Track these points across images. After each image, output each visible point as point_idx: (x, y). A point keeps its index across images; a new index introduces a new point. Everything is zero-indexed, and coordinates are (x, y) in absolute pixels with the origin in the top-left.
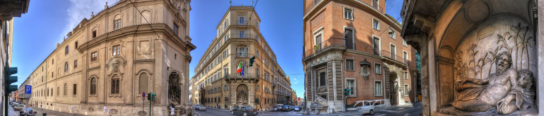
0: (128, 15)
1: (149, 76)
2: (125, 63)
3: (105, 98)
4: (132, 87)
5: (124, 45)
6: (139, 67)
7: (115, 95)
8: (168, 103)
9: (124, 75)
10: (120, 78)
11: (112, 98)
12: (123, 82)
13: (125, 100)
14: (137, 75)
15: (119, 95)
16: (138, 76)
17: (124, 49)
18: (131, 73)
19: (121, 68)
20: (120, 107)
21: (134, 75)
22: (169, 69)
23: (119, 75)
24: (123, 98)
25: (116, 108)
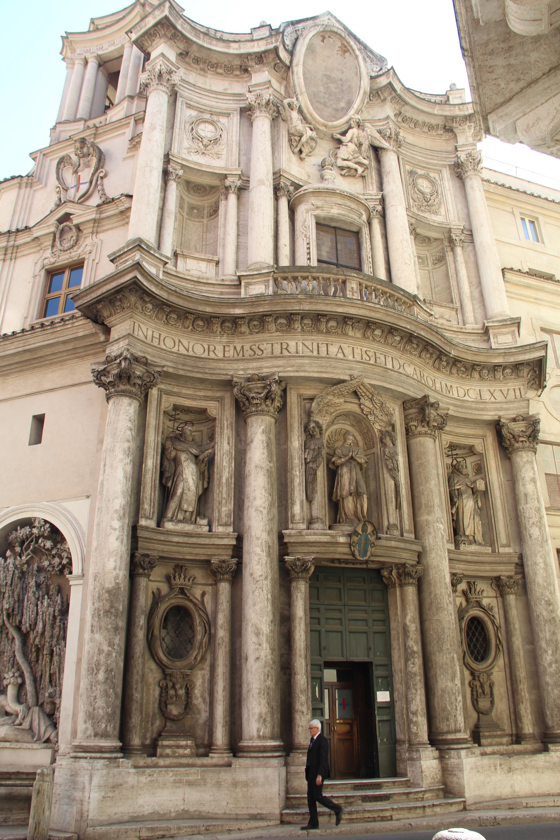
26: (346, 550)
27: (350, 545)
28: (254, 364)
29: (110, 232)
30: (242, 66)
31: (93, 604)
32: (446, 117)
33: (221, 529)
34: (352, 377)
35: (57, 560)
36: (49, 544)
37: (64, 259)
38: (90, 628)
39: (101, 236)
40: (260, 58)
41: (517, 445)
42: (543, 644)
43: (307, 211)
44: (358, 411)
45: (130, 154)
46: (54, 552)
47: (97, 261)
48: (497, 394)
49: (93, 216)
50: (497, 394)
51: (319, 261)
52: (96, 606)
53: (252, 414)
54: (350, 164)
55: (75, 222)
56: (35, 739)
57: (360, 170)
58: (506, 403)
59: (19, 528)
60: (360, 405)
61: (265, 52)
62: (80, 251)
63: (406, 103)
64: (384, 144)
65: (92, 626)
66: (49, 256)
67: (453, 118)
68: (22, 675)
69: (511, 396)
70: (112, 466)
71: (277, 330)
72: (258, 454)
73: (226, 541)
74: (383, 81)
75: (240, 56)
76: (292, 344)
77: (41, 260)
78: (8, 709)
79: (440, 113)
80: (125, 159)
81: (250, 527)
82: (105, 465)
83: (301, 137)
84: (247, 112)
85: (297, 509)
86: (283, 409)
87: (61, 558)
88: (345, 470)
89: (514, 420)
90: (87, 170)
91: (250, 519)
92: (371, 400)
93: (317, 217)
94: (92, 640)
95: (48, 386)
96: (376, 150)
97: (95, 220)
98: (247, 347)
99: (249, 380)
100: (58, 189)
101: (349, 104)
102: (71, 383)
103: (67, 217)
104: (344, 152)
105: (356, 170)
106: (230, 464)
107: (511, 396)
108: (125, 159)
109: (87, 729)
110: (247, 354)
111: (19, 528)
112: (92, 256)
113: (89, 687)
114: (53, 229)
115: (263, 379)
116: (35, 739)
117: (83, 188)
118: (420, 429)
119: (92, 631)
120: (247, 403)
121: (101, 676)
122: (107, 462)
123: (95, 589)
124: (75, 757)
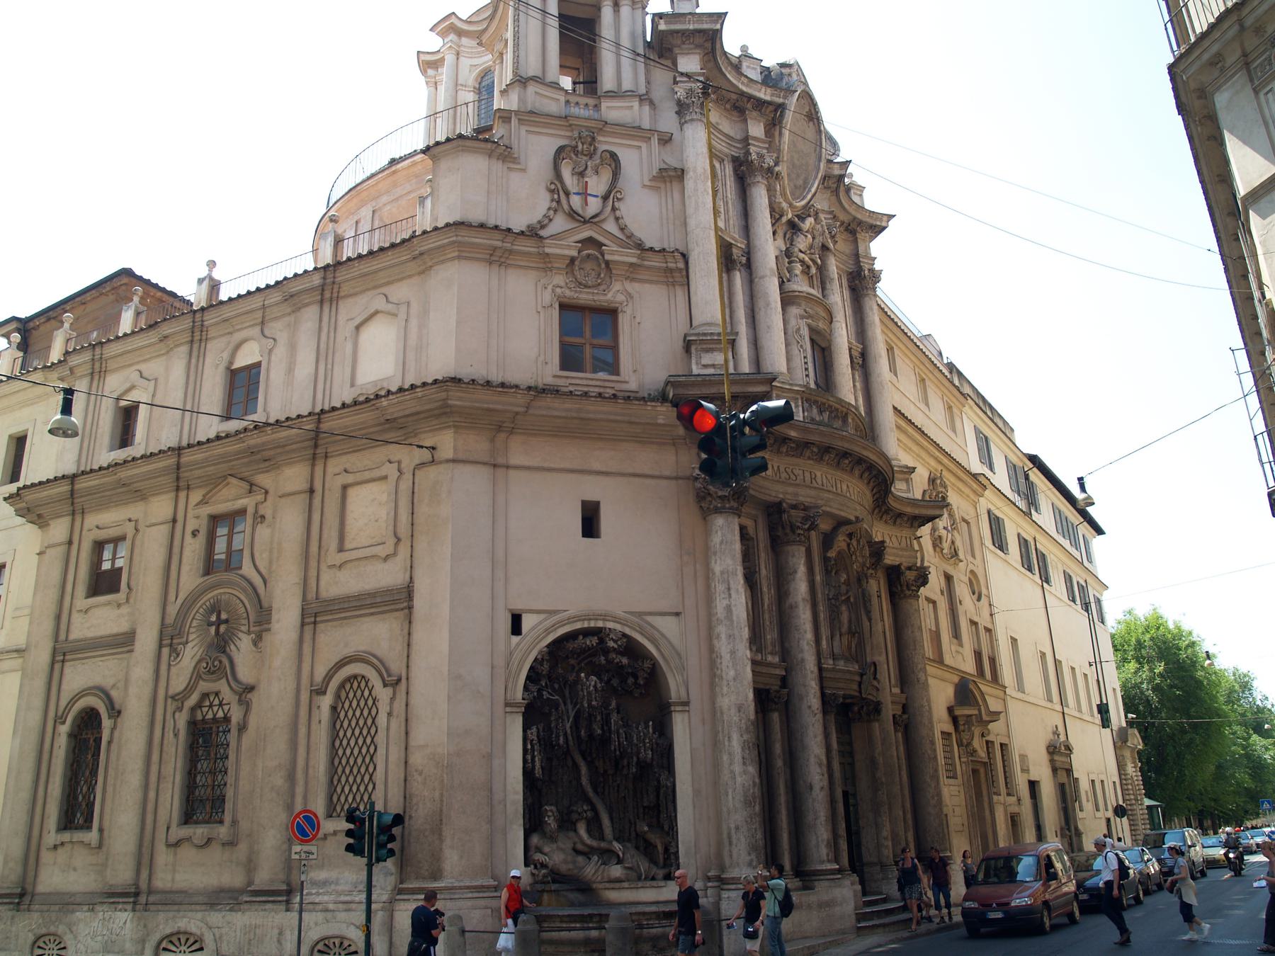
0: (293, 347)
1: (383, 694)
2: (263, 616)
3: (144, 858)
4: (291, 778)
5: (266, 510)
6: (337, 641)
7: (200, 832)
9: (254, 697)
10: (236, 715)
11: (187, 852)
12: (247, 739)
13: (250, 866)
14: (322, 692)
15: (223, 831)
16: (326, 701)
17: (263, 532)
18: (291, 685)
19: (243, 649)
20: (215, 918)
21: (305, 696)
22: (527, 622)
23: (227, 694)
24: (243, 848)
25: (191, 922)
26: (855, 687)
27: (860, 684)
28: (790, 489)
29: (647, 286)
30: (740, 105)
32: (855, 218)
33: (770, 658)
34: (857, 518)
35: (631, 680)
36: (625, 661)
37: (585, 297)
39: (637, 286)
40: (760, 104)
41: (908, 593)
42: (928, 780)
43: (802, 317)
44: (845, 548)
45: (653, 184)
47: (638, 320)
48: (894, 539)
49: (634, 260)
50: (894, 539)
51: (816, 383)
52: (746, 737)
53: (789, 543)
54: (807, 259)
55: (607, 257)
57: (813, 270)
58: (902, 549)
60: (848, 545)
61: (770, 103)
62: (609, 296)
63: (838, 196)
64: (831, 246)
66: (563, 284)
67: (860, 223)
68: (594, 809)
69: (903, 544)
70: (737, 591)
71: (809, 458)
72: (800, 588)
73: (778, 672)
74: (837, 172)
75: (742, 94)
76: (819, 474)
77: (550, 287)
78: (579, 847)
79: (853, 213)
80: (644, 186)
81: (803, 660)
82: (729, 589)
83: (781, 216)
84: (744, 171)
85: (824, 643)
86: (809, 539)
87: (636, 677)
88: (844, 608)
89: (909, 568)
90: (595, 177)
91: (802, 651)
92: (858, 542)
93: (809, 326)
94: (745, 772)
95: (597, 466)
96: (824, 248)
97: (632, 265)
98: (782, 469)
99: (794, 507)
100: (553, 187)
101: (805, 186)
102: (631, 471)
103: (590, 242)
104: (802, 243)
105: (808, 267)
106: (769, 590)
107: (903, 544)
108: (644, 186)
109: (752, 861)
110: (784, 475)
112: (629, 310)
114: (574, 253)
115: (806, 509)
117: (594, 205)
118: (870, 571)
119: (744, 764)
120: (788, 531)
121: (757, 808)
122: (732, 586)
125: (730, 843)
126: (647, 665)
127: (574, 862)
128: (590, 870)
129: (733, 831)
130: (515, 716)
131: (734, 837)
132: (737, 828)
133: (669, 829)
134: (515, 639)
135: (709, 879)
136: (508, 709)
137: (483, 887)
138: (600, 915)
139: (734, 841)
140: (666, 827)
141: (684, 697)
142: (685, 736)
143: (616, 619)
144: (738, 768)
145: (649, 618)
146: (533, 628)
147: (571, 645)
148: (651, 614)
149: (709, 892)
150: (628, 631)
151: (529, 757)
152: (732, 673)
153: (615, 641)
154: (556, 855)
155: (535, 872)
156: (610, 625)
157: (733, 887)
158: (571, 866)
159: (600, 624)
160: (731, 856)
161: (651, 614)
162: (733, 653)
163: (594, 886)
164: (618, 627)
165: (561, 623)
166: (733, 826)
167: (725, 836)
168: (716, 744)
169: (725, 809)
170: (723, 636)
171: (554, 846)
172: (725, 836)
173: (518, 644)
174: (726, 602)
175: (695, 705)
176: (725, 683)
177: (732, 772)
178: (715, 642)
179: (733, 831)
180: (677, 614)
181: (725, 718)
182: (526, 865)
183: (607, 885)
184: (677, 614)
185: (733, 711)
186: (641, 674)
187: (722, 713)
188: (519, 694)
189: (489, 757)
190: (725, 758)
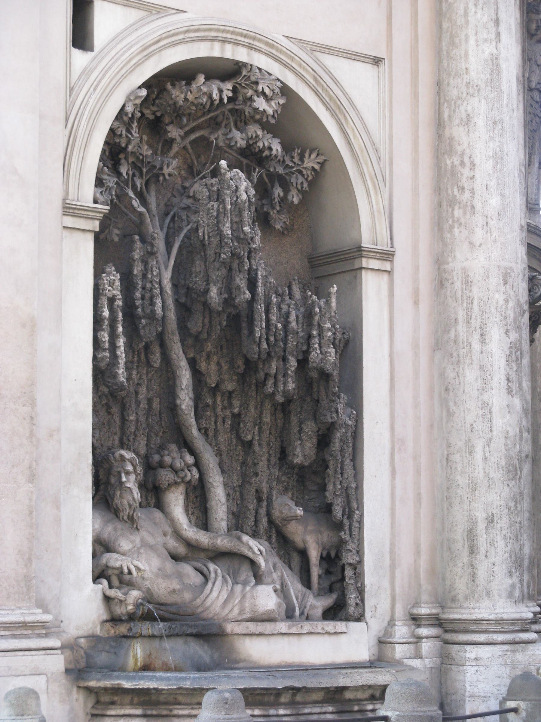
8: (82, 607)
31: (507, 333)
38: (504, 383)
46: (280, 170)
52: (514, 336)
56: (297, 613)
59: (201, 79)
65: (508, 380)
82: (497, 22)
87: (286, 186)
109: (513, 586)
111: (201, 79)
113: (512, 504)
116: (297, 613)
119: (509, 391)
123: (507, 301)
124: (514, 643)
125: (473, 550)
126: (311, 162)
127: (180, 576)
128: (218, 597)
129: (481, 526)
130: (78, 235)
131: (482, 540)
132: (490, 520)
133: (340, 517)
134: (80, 58)
135: (416, 620)
136: (69, 221)
137: (25, 625)
138: (296, 690)
139: (483, 550)
140: (338, 511)
141: (384, 245)
142: (387, 321)
143: (272, 50)
144: (498, 398)
145: (329, 61)
146: (117, 38)
147: (178, 94)
148: (331, 50)
149: (426, 646)
150: (292, 81)
151: (105, 336)
152: (495, 202)
153: (268, 99)
154: (145, 560)
155: (112, 593)
156: (260, 61)
157: (482, 638)
158: (175, 585)
159: (241, 55)
160: (473, 577)
161: (331, 50)
162: (498, 159)
163: (229, 628)
164: (276, 70)
165: (174, 39)
166: (480, 515)
167: (459, 533)
168: (443, 342)
169: (462, 480)
170: (480, 122)
171: (137, 539)
172: (459, 533)
173: (86, 72)
174: (489, 49)
175: (402, 261)
176: (479, 220)
177: (485, 405)
178: (457, 132)
179: (481, 526)
180: (377, 61)
181: (476, 293)
182: (96, 579)
183: (252, 627)
184: (377, 61)
185: (495, 281)
186: (297, 180)
187: (468, 283)
188: (86, 192)
189: (31, 327)
190: (471, 375)
